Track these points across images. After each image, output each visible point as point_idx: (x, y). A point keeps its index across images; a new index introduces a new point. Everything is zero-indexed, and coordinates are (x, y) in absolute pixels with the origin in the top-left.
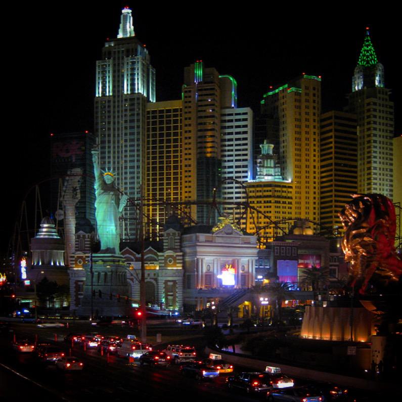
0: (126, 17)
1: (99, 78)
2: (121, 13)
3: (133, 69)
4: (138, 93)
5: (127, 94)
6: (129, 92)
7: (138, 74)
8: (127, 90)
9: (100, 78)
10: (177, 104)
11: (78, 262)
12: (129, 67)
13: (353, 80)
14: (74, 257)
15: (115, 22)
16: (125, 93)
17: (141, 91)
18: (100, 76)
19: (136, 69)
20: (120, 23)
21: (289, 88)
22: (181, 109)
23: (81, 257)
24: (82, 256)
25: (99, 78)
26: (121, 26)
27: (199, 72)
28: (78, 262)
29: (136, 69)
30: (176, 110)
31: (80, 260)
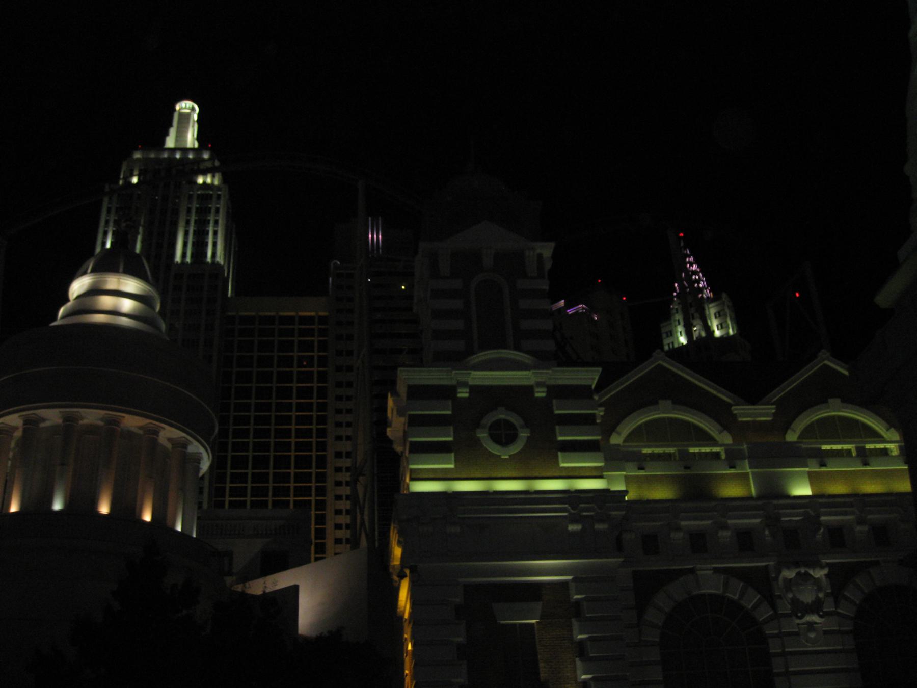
0: (185, 118)
1: (107, 222)
2: (174, 110)
3: (203, 213)
4: (214, 263)
5: (183, 262)
6: (188, 260)
7: (216, 222)
8: (184, 255)
9: (111, 224)
10: (312, 308)
11: (483, 435)
12: (195, 205)
13: (664, 330)
14: (446, 393)
15: (164, 120)
16: (178, 258)
17: (220, 259)
18: (113, 217)
19: (213, 211)
20: (171, 125)
21: (568, 305)
22: (323, 320)
23: (515, 397)
24: (529, 390)
25: (107, 222)
26: (173, 132)
27: (376, 237)
28: (482, 435)
29: (213, 211)
30: (310, 320)
31: (502, 415)
